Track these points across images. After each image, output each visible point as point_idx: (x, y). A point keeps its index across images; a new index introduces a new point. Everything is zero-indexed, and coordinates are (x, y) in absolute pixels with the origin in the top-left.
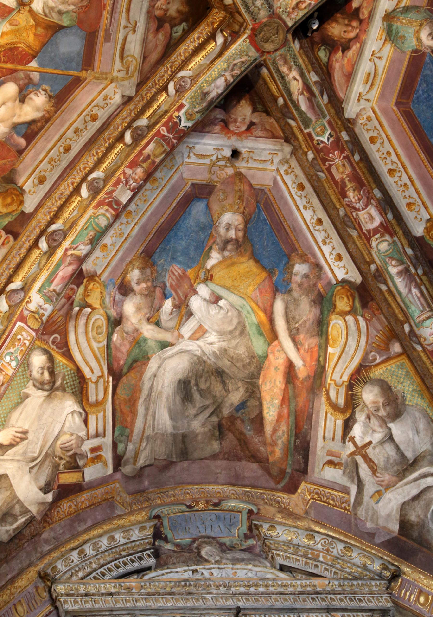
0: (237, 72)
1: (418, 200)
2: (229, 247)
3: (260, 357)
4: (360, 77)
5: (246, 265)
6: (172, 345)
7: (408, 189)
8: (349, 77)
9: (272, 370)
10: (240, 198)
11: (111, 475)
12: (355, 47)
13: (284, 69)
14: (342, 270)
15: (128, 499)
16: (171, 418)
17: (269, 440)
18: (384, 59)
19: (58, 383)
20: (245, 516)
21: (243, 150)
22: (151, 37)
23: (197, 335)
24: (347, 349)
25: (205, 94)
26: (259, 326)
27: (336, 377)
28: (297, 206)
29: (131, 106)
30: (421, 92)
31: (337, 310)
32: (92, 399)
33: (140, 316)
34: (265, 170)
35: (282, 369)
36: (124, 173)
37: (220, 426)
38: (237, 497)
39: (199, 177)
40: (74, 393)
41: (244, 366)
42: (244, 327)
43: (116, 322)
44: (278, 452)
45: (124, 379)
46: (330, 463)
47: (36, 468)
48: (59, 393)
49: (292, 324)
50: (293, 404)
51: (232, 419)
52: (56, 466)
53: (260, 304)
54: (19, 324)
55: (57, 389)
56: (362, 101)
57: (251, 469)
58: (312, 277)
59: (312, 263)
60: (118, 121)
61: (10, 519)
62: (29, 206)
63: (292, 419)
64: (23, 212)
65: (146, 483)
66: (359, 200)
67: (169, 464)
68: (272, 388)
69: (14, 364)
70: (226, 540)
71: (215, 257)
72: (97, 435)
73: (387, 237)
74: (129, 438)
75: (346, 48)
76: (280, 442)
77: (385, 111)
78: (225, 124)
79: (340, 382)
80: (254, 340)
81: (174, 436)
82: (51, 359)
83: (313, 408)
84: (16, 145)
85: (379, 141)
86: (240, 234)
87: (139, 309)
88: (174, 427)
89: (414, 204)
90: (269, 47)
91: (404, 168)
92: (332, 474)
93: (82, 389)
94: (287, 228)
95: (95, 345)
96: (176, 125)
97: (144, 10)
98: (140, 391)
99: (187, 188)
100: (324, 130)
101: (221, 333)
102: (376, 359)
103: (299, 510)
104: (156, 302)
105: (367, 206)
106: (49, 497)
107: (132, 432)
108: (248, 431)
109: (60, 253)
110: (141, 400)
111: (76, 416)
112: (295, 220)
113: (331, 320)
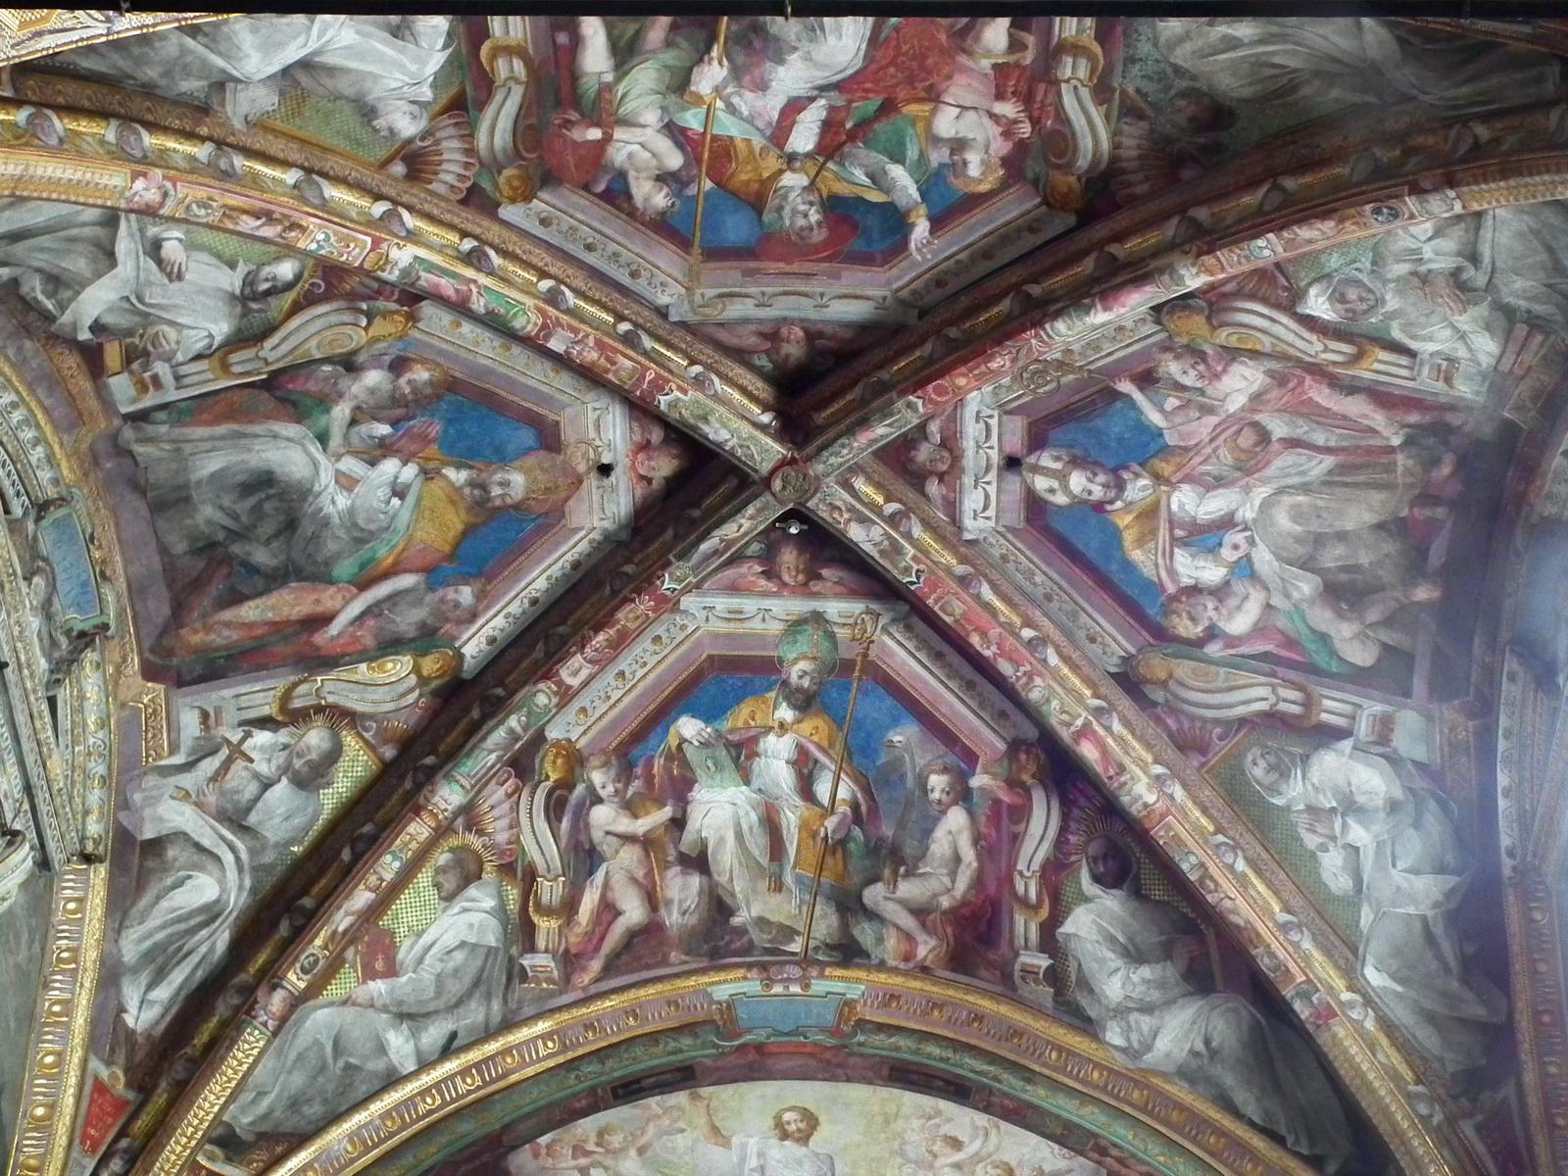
0: (739, 452)
2: (477, 492)
4: (735, 602)
8: (734, 589)
10: (547, 489)
11: (117, 412)
12: (772, 587)
13: (750, 510)
14: (474, 646)
15: (84, 446)
16: (213, 475)
17: (211, 621)
19: (254, 306)
20: (97, 621)
21: (613, 478)
22: (753, 327)
23: (343, 480)
25: (705, 419)
29: (657, 321)
32: (234, 358)
33: (362, 396)
34: (590, 511)
35: (319, 609)
36: (587, 336)
37: (212, 545)
38: (119, 597)
39: (569, 430)
40: (239, 331)
42: (368, 541)
43: (349, 364)
44: (197, 639)
45: (264, 395)
46: (205, 715)
47: (127, 306)
48: (239, 309)
51: (228, 560)
52: (130, 333)
54: (369, 240)
55: (244, 306)
57: (160, 608)
60: (636, 307)
61: (50, 288)
62: (508, 212)
64: (498, 205)
65: (109, 465)
67: (139, 488)
68: (288, 603)
69: (314, 246)
70: (57, 606)
71: (457, 476)
72: (178, 378)
73: (555, 700)
74: (176, 422)
75: (768, 574)
76: (212, 637)
77: (698, 643)
78: (645, 447)
81: (186, 486)
82: (289, 286)
84: (595, 181)
86: (498, 502)
87: (372, 391)
88: (199, 482)
90: (777, 484)
92: (190, 723)
93: (247, 340)
95: (313, 342)
96: (660, 390)
97: (787, 313)
98: (250, 422)
99: (552, 417)
100: (679, 580)
101: (351, 511)
103: (124, 694)
104: (385, 413)
105: (590, 662)
106: (84, 335)
107: (186, 425)
108: (216, 588)
109: (469, 273)
110: (235, 427)
111: (206, 341)
112: (531, 571)
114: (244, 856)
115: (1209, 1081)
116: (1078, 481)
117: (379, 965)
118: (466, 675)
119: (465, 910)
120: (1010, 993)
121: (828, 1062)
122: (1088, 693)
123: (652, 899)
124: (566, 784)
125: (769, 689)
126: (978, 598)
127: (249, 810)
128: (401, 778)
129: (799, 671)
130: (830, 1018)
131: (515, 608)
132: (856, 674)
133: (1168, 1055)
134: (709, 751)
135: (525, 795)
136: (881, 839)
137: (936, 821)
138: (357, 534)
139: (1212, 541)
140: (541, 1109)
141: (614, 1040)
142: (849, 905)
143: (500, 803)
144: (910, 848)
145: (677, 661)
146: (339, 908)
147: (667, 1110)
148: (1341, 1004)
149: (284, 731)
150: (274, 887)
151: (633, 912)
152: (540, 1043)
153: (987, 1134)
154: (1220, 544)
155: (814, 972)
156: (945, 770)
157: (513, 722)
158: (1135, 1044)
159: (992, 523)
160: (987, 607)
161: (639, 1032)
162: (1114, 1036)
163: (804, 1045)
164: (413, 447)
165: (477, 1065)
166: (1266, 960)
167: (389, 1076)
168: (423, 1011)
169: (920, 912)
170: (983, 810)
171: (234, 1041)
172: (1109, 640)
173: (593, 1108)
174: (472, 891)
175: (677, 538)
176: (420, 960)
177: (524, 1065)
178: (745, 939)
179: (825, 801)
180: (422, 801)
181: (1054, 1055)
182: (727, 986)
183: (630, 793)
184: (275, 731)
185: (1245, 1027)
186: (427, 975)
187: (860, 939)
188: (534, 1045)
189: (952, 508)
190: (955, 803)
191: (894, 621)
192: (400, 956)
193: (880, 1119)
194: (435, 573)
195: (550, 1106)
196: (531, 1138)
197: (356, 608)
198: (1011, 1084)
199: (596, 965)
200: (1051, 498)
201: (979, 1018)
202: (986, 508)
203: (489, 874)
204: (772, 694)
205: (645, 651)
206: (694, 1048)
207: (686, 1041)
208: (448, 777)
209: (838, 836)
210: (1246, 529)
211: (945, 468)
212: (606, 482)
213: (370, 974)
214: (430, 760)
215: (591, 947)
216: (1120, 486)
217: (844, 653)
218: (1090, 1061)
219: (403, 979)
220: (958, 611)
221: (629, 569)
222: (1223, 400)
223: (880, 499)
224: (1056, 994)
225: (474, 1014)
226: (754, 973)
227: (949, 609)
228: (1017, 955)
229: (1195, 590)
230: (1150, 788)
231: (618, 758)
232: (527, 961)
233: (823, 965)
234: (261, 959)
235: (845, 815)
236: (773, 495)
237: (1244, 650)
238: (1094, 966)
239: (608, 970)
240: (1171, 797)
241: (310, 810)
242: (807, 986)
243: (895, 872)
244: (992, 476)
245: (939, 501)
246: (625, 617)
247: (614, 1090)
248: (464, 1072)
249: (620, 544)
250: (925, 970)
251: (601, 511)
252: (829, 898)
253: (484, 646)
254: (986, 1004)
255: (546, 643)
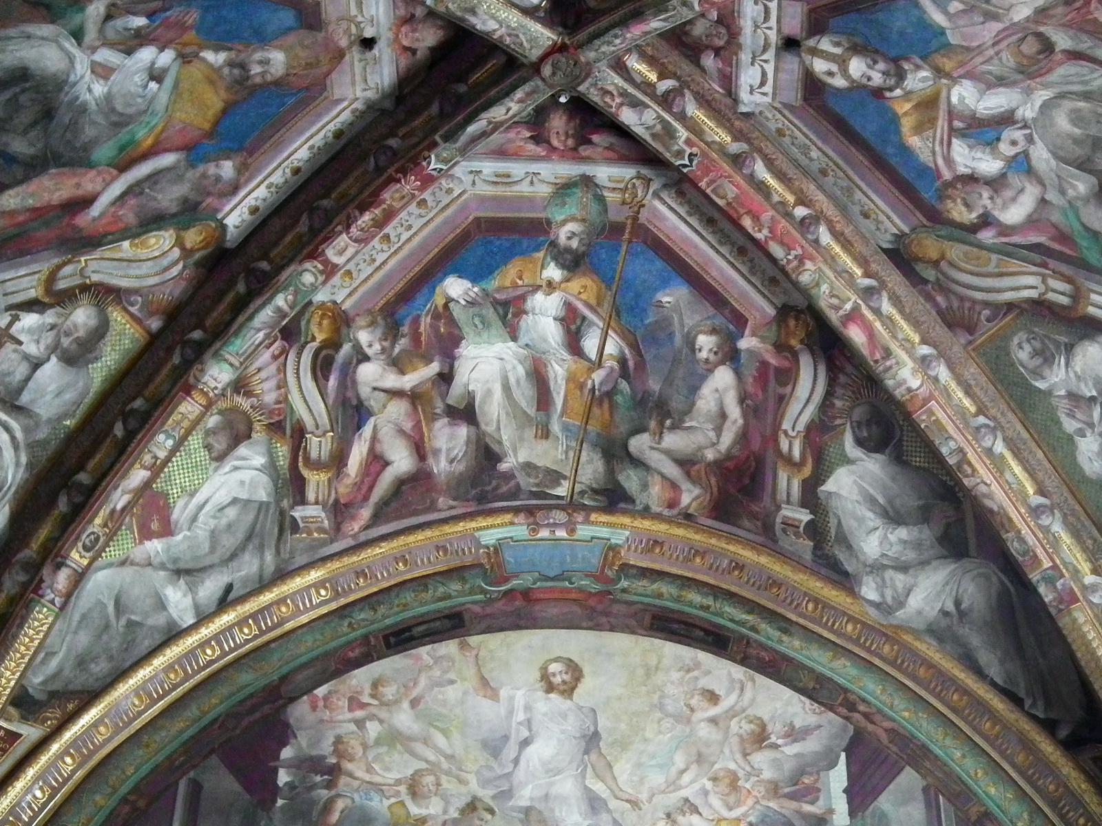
1: (358, 282)
2: (236, 71)
3: (88, 158)
5: (215, 99)
6: (79, 44)
7: (369, 265)
8: (501, 153)
9: (75, 180)
10: (309, 65)
12: (540, 150)
14: (236, 217)
18: (531, 189)
21: (376, 51)
23: (99, 70)
24: (134, 265)
26: (132, 142)
27: (93, 266)
28: (312, 137)
30: (498, 243)
31: (182, 233)
34: (353, 83)
35: (80, 192)
41: (69, 142)
42: (127, 124)
49: (146, 185)
50: (35, 224)
53: (164, 135)
56: (471, 177)
58: (219, 186)
59: (238, 180)
63: (15, 231)
66: (362, 230)
68: (51, 189)
71: (215, 58)
73: (321, 278)
75: (537, 139)
77: (464, 208)
78: (409, 20)
79: (88, 272)
80: (111, 143)
83: (39, 252)
85: (422, 211)
86: (258, 80)
89: (351, 278)
91: (396, 252)
94: (279, 135)
101: (108, 98)
102: (132, 305)
105: (356, 241)
112: (292, 141)
113: (166, 230)
114: (19, 435)
115: (958, 641)
116: (857, 67)
117: (155, 526)
118: (228, 245)
119: (236, 468)
120: (769, 543)
121: (593, 609)
122: (858, 272)
123: (420, 449)
124: (333, 344)
125: (537, 249)
126: (751, 178)
127: (20, 390)
128: (170, 351)
129: (568, 233)
130: (595, 561)
131: (277, 178)
132: (626, 236)
133: (919, 613)
134: (476, 310)
135: (292, 356)
136: (646, 394)
137: (703, 378)
138: (114, 118)
139: (991, 135)
140: (317, 658)
141: (385, 585)
142: (615, 452)
143: (267, 365)
144: (676, 403)
145: (445, 222)
146: (116, 488)
147: (437, 660)
148: (1084, 588)
149: (50, 312)
150: (48, 460)
151: (401, 461)
152: (313, 591)
153: (742, 690)
154: (998, 139)
155: (580, 519)
156: (713, 331)
157: (280, 301)
158: (889, 600)
159: (768, 99)
160: (762, 188)
161: (409, 576)
162: (869, 591)
163: (569, 591)
164: (171, 34)
165: (253, 616)
166: (1016, 544)
167: (170, 630)
168: (201, 565)
169: (686, 463)
170: (750, 372)
171: (24, 620)
172: (882, 217)
173: (366, 659)
174: (242, 450)
175: (444, 116)
176: (194, 519)
177: (298, 612)
178: (513, 483)
179: (593, 355)
180: (192, 380)
181: (810, 606)
182: (493, 531)
183: (397, 350)
184: (41, 312)
185: (994, 592)
186: (202, 531)
187: (626, 485)
188: (307, 594)
189: (728, 82)
190: (722, 363)
191: (665, 186)
192: (175, 515)
193: (640, 672)
194: (195, 150)
195: (326, 655)
196: (309, 691)
197: (117, 189)
198: (768, 634)
199: (366, 513)
200: (829, 80)
201: (740, 567)
202: (763, 84)
203: (259, 435)
204: (541, 254)
205: (410, 214)
206: (462, 593)
207: (455, 586)
208: (216, 355)
209: (605, 389)
210: (1025, 127)
211: (721, 43)
212: (369, 55)
213: (146, 534)
214: (197, 335)
215: (360, 497)
216: (901, 76)
217: (615, 215)
218: (844, 614)
219: (179, 537)
220: (730, 195)
221: (393, 142)
222: (1008, 10)
223: (653, 77)
224: (816, 548)
225: (249, 566)
226: (521, 518)
227: (721, 192)
228: (779, 508)
229: (972, 179)
230: (914, 372)
231: (384, 318)
232: (298, 513)
233: (587, 510)
234: (43, 533)
235: (612, 369)
236: (543, 80)
237: (1016, 239)
238: (854, 524)
239: (378, 517)
240: (936, 380)
241: (81, 384)
242: (572, 531)
243: (661, 424)
244: (770, 55)
245: (715, 74)
246: (389, 196)
247: (386, 637)
248: (242, 623)
249: (383, 112)
250: (688, 517)
251: (362, 83)
252: (595, 445)
253: (246, 216)
254: (747, 554)
255: (310, 218)
